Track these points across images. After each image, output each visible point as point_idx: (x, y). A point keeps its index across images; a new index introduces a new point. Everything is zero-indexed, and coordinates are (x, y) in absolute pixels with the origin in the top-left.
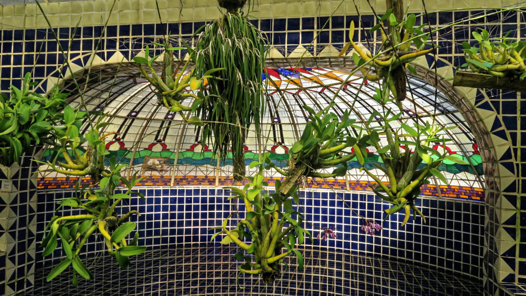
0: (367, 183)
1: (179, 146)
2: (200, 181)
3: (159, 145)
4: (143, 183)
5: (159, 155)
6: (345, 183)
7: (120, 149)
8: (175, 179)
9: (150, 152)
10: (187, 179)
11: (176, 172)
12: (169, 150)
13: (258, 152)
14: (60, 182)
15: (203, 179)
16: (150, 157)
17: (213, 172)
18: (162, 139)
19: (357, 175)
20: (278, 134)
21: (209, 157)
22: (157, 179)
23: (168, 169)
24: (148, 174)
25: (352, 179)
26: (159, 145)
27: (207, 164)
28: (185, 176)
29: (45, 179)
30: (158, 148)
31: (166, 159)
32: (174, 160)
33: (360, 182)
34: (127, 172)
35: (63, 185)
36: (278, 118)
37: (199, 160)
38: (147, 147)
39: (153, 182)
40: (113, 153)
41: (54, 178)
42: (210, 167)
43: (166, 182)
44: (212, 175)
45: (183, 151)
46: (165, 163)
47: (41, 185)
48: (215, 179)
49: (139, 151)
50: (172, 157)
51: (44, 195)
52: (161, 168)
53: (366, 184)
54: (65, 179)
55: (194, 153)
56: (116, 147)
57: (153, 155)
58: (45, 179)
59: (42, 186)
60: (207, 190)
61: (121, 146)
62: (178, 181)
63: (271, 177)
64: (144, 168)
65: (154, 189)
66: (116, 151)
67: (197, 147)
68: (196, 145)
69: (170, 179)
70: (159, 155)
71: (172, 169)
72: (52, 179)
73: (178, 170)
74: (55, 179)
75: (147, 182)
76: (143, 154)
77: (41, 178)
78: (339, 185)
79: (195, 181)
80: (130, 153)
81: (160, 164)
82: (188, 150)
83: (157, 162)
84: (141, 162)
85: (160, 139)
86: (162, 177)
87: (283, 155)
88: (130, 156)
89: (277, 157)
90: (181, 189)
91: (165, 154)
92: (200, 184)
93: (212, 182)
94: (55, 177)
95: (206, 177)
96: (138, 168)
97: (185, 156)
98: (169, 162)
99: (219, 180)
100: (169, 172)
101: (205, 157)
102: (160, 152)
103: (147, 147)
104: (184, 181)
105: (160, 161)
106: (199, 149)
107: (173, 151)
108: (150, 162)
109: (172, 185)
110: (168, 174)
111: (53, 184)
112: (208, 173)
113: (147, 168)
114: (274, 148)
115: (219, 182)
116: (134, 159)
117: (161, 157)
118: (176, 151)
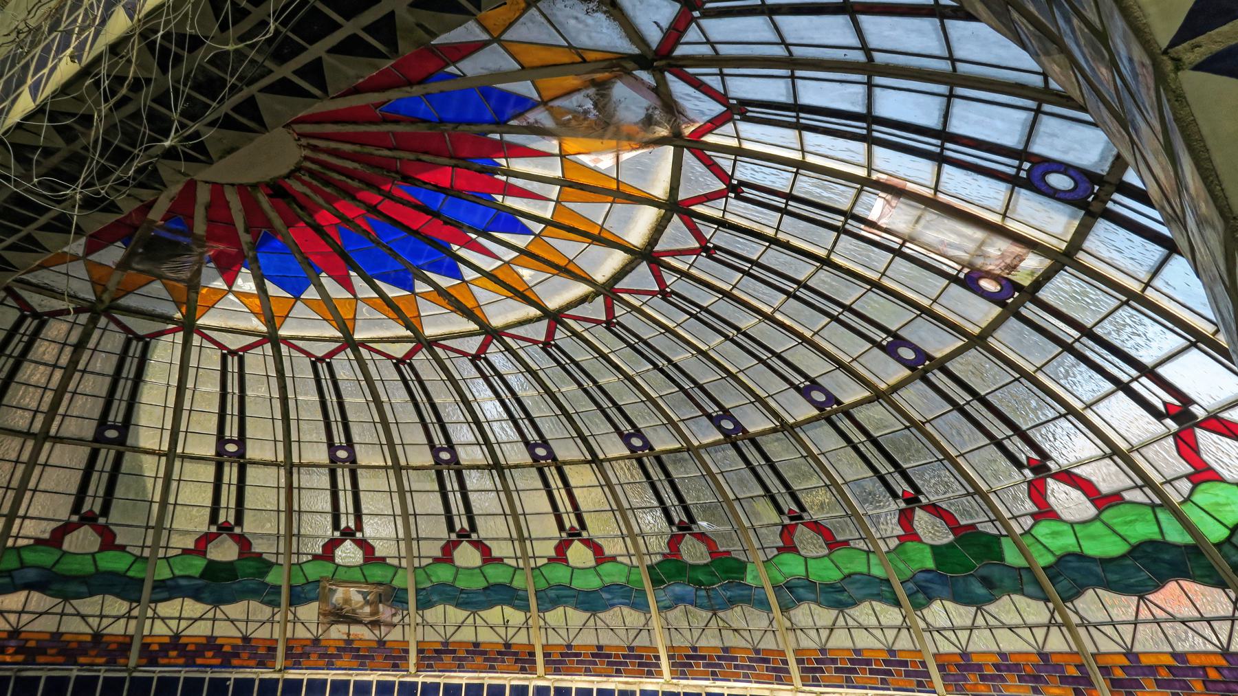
0: (998, 660)
1: (409, 549)
2: (477, 654)
3: (348, 543)
4: (329, 661)
5: (358, 575)
6: (923, 664)
7: (240, 554)
8: (420, 651)
9: (331, 567)
10: (454, 652)
11: (420, 629)
12: (383, 559)
13: (635, 561)
14: (74, 645)
15: (499, 653)
16: (335, 580)
17: (524, 631)
18: (352, 525)
19: (953, 629)
20: (670, 499)
21: (501, 580)
22: (369, 649)
23: (396, 619)
24: (338, 632)
25: (945, 647)
26: (348, 543)
27: (502, 602)
28: (446, 643)
29: (23, 636)
30: (348, 553)
31: (381, 589)
32: (406, 590)
33: (975, 660)
34: (277, 627)
35: (85, 654)
36: (638, 433)
37: (475, 592)
38: (319, 551)
39: (357, 657)
40: (215, 571)
41: (52, 634)
42: (515, 616)
43: (396, 658)
44: (521, 638)
45: (425, 562)
46: (380, 599)
47: (11, 651)
48: (532, 654)
49: (299, 564)
50: (397, 583)
51: (9, 678)
52: (372, 614)
53: (997, 667)
54: (89, 638)
55: (458, 568)
56: (224, 551)
57: (341, 575)
58: (23, 636)
59: (16, 653)
60: (504, 686)
61: (241, 549)
62: (433, 656)
63: (694, 649)
64: (325, 615)
65: (353, 679)
66: (231, 563)
67: (459, 549)
68: (456, 544)
69: (407, 651)
70: (358, 575)
71: (407, 620)
72: (47, 637)
73: (425, 624)
74: (57, 635)
75: (339, 657)
76: (314, 571)
77: (9, 632)
78: (908, 674)
79: (479, 660)
80: (275, 569)
81: (367, 603)
82: (437, 560)
83: (357, 598)
84: (312, 595)
85: (348, 528)
86: (381, 643)
87: (706, 565)
88: (271, 578)
89: (692, 574)
90: (429, 680)
91: (377, 573)
92: (492, 669)
93: (523, 660)
94: (54, 630)
95: (507, 645)
96: (309, 612)
97: (434, 579)
98: (396, 597)
99: (546, 655)
100: (399, 628)
101: (492, 581)
102: (360, 566)
103: (319, 551)
104: (447, 659)
105: (365, 595)
106: (467, 556)
107: (395, 562)
108: (339, 595)
109: (412, 669)
110: (395, 635)
111: (50, 651)
112: (511, 632)
113: (331, 613)
114: (674, 542)
115: (546, 663)
116: (291, 587)
117: (367, 582)
118: (404, 563)
